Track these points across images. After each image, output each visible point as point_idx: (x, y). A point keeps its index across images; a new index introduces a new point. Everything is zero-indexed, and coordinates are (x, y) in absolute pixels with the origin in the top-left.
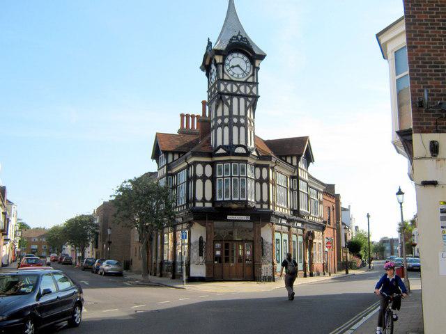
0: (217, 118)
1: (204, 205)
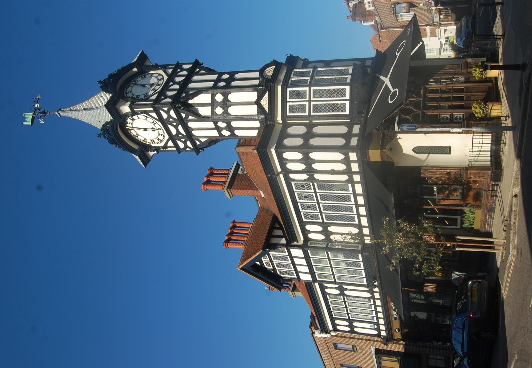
0: (214, 118)
1: (355, 135)
